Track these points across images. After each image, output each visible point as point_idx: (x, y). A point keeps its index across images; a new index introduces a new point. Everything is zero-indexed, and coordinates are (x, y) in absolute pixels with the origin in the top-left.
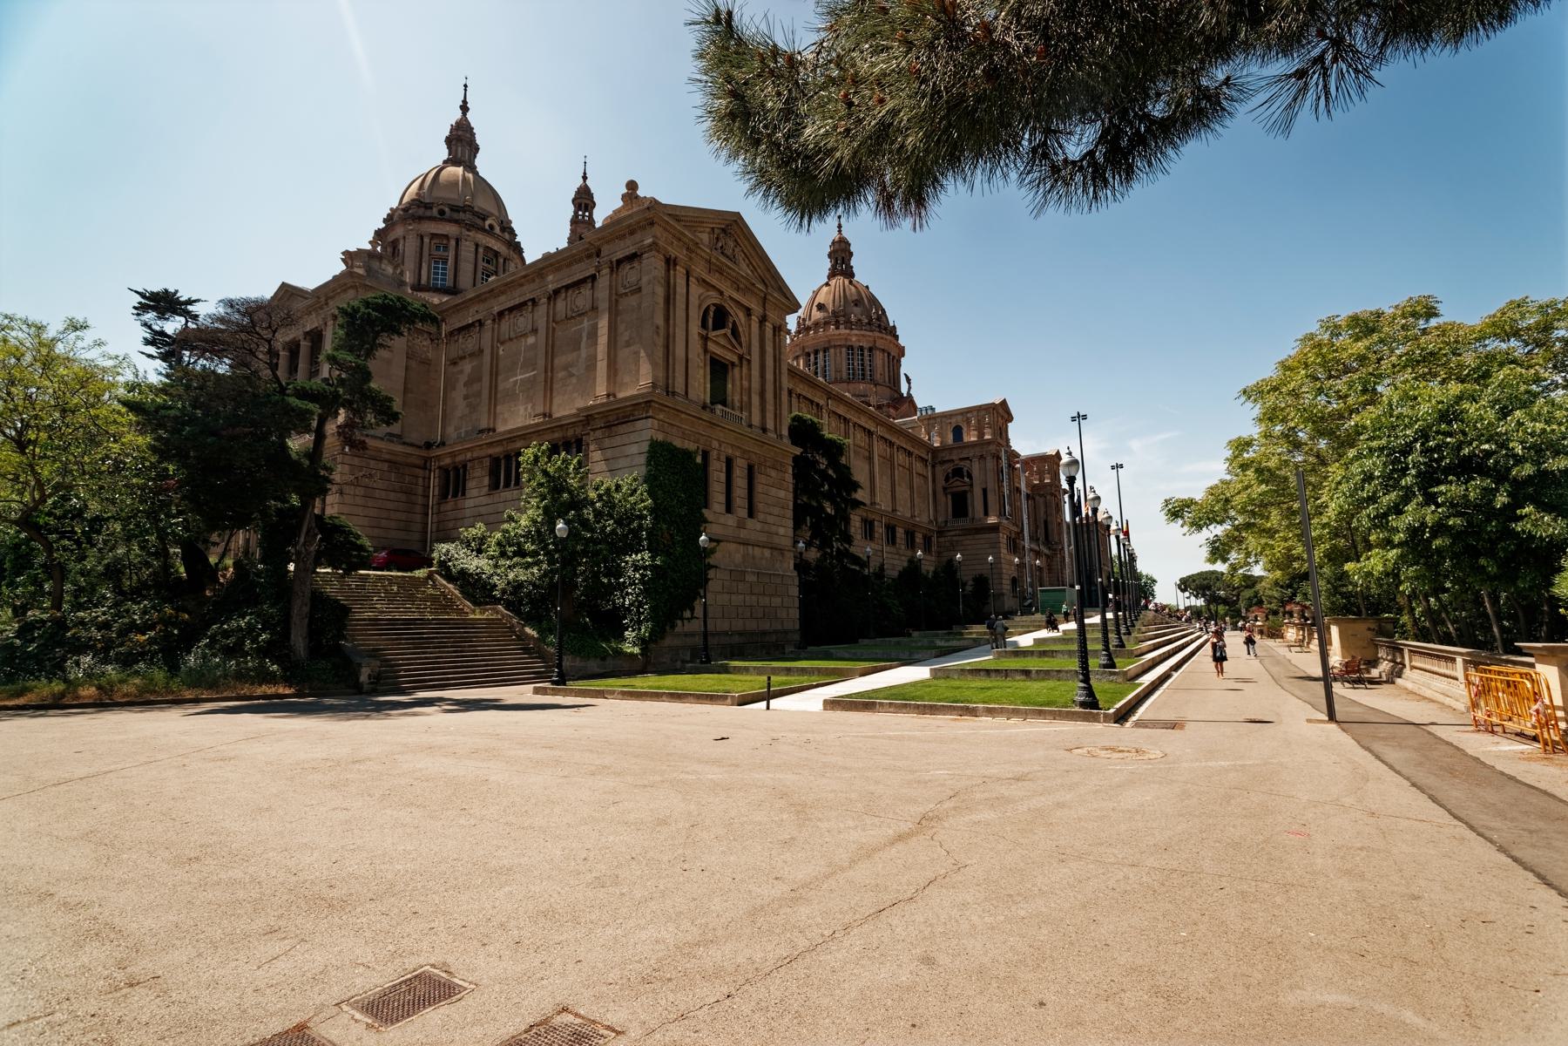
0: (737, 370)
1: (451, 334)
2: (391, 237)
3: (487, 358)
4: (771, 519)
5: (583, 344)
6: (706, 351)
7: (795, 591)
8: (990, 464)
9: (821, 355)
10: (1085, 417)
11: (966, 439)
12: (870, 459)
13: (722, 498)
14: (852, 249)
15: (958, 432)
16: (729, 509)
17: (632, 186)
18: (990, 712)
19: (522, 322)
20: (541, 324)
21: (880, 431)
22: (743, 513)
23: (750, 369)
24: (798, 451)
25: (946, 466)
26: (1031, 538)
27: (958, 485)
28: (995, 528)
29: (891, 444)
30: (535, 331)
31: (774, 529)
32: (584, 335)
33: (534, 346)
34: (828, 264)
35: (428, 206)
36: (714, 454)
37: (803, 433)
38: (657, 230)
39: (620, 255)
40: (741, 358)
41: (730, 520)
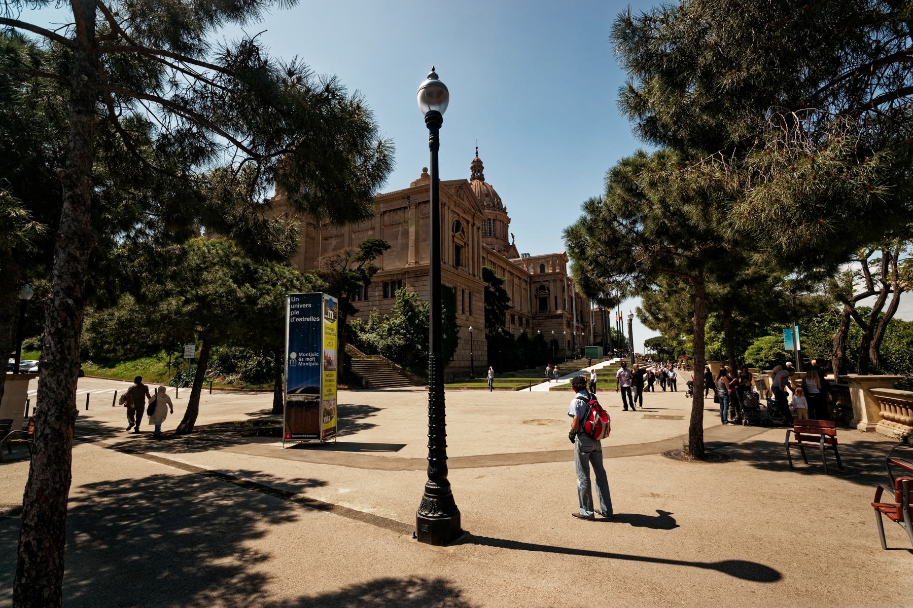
4: (477, 316)
5: (399, 238)
7: (486, 348)
8: (559, 284)
11: (546, 271)
16: (463, 313)
18: (607, 390)
20: (377, 226)
21: (508, 268)
22: (468, 314)
24: (486, 284)
26: (577, 321)
27: (542, 294)
28: (561, 316)
29: (513, 274)
37: (488, 275)
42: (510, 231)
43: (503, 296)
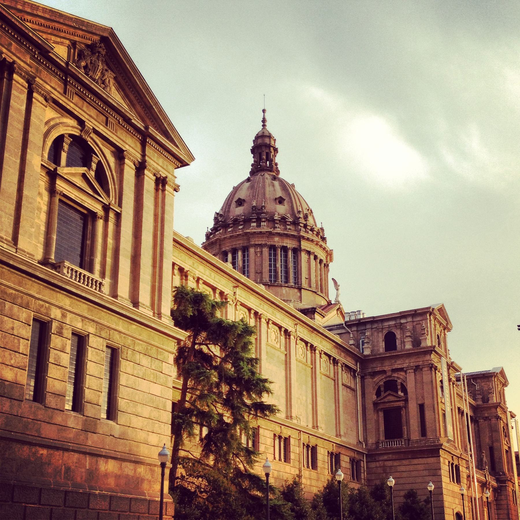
9: (240, 253)
15: (390, 340)
27: (390, 400)
29: (313, 348)
34: (250, 159)
40: (106, 208)
42: (330, 276)
43: (245, 384)
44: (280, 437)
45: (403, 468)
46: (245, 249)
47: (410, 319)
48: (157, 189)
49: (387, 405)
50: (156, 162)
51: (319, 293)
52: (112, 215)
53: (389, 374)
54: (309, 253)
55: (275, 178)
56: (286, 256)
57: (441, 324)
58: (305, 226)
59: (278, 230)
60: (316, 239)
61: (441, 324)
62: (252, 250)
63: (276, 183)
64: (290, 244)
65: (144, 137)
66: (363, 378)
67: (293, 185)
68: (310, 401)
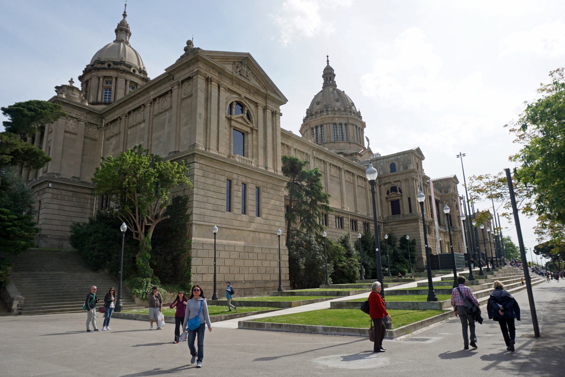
0: (250, 136)
1: (107, 125)
2: (86, 79)
3: (122, 135)
4: (271, 217)
5: (166, 126)
6: (231, 126)
9: (319, 128)
10: (464, 155)
12: (340, 183)
13: (240, 206)
14: (335, 73)
15: (393, 167)
16: (244, 212)
17: (189, 43)
19: (138, 116)
21: (346, 167)
22: (253, 214)
23: (257, 135)
24: (288, 179)
25: (387, 186)
27: (394, 196)
30: (144, 121)
31: (272, 223)
32: (167, 122)
33: (144, 128)
35: (103, 63)
36: (234, 182)
38: (200, 65)
39: (183, 78)
40: (252, 129)
41: (245, 218)
42: (365, 135)
44: (338, 217)
45: (401, 228)
46: (321, 126)
47: (402, 156)
48: (273, 117)
49: (392, 199)
50: (271, 106)
51: (359, 143)
52: (254, 132)
53: (393, 183)
54: (353, 125)
55: (334, 89)
56: (342, 128)
57: (418, 157)
58: (350, 112)
59: (337, 115)
60: (356, 117)
61: (418, 157)
62: (325, 126)
63: (335, 92)
64: (343, 121)
65: (266, 97)
66: (380, 186)
67: (344, 92)
68: (353, 199)
